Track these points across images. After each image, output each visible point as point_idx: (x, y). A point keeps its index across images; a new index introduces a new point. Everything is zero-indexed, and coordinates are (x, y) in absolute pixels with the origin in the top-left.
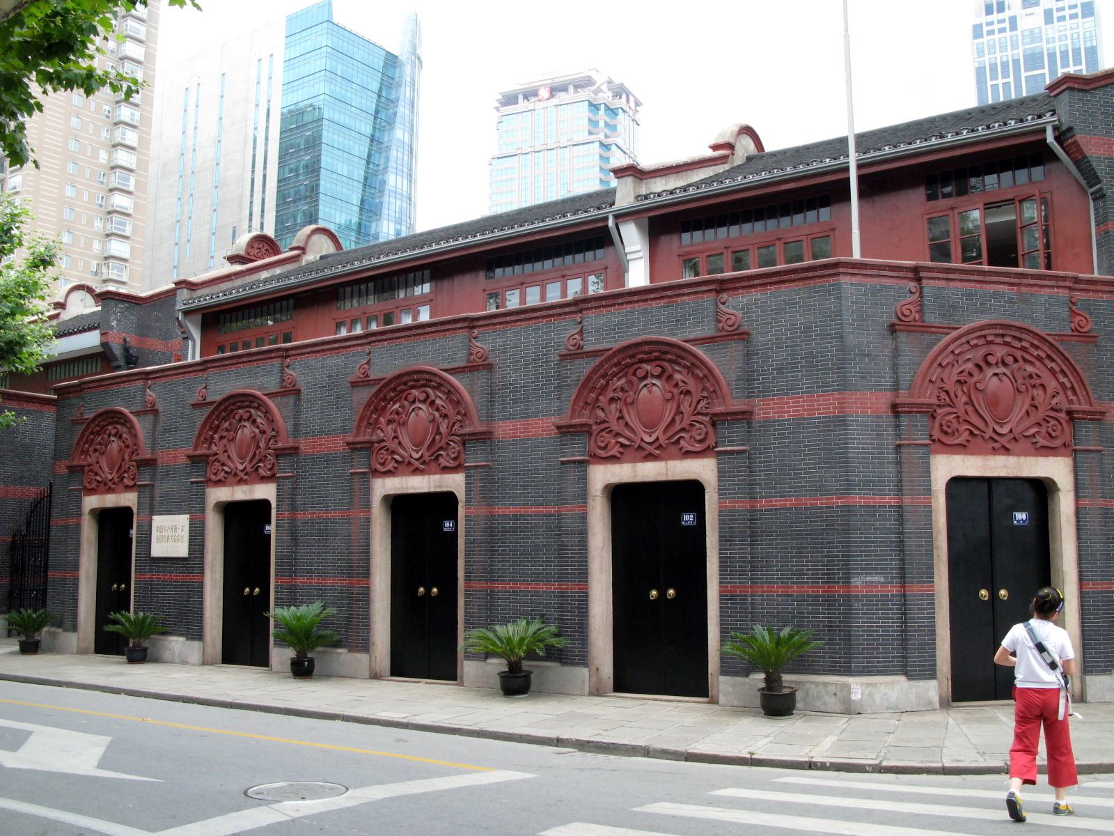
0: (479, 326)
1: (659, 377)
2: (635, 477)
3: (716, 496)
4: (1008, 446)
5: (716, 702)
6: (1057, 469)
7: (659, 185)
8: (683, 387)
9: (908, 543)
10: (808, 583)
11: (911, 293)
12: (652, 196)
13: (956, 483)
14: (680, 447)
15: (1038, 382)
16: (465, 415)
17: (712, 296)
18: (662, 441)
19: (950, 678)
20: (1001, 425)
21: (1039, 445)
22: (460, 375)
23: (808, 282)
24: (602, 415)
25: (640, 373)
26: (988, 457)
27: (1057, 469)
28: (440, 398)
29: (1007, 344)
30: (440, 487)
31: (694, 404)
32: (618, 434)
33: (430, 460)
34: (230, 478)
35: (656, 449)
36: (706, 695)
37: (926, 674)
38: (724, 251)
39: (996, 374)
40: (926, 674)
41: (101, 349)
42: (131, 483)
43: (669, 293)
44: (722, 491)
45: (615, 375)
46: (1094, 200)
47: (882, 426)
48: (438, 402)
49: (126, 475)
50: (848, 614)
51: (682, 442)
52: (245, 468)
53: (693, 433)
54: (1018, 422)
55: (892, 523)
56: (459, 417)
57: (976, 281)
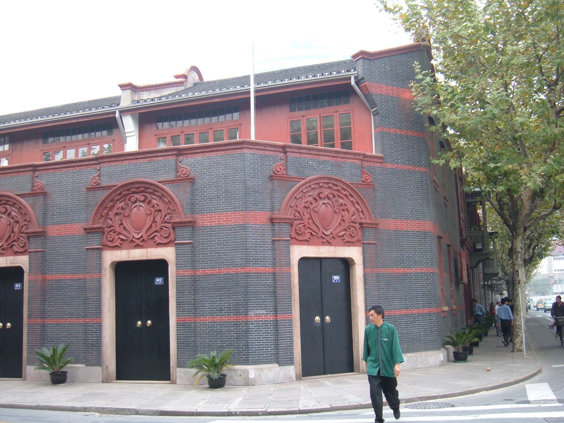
0: (39, 170)
1: (143, 202)
2: (129, 257)
3: (175, 268)
4: (330, 241)
5: (175, 383)
7: (145, 96)
8: (158, 208)
9: (279, 292)
10: (225, 315)
11: (282, 159)
12: (141, 101)
13: (304, 261)
14: (155, 241)
15: (345, 208)
16: (29, 221)
17: (174, 157)
18: (145, 237)
19: (301, 364)
20: (327, 230)
21: (345, 241)
22: (27, 198)
23: (226, 152)
24: (111, 222)
25: (133, 199)
28: (15, 211)
29: (330, 188)
30: (13, 263)
31: (163, 217)
32: (119, 233)
33: (7, 248)
35: (141, 242)
36: (169, 379)
37: (288, 363)
38: (181, 134)
39: (324, 204)
40: (288, 363)
43: (150, 155)
44: (178, 265)
45: (118, 200)
46: (374, 115)
47: (265, 230)
48: (13, 214)
50: (247, 331)
51: (156, 238)
53: (162, 233)
55: (271, 281)
56: (26, 223)
57: (315, 155)
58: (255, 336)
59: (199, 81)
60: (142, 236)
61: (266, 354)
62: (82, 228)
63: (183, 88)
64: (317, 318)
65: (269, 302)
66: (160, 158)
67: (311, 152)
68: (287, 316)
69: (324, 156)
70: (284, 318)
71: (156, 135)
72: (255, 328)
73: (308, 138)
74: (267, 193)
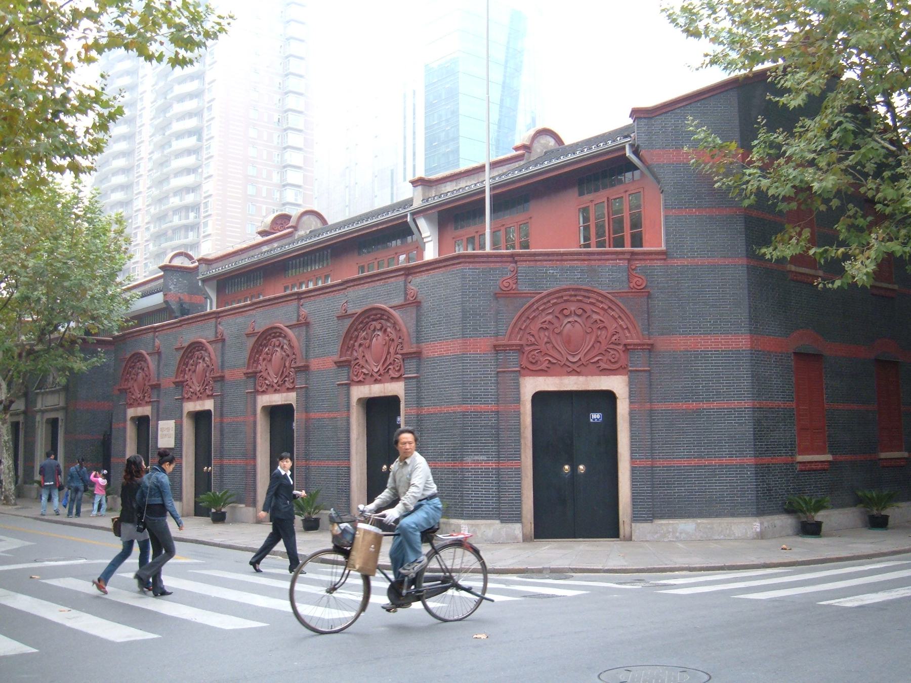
4: (578, 370)
6: (617, 384)
7: (449, 187)
13: (540, 398)
15: (601, 325)
19: (533, 522)
20: (574, 356)
21: (601, 368)
22: (294, 329)
23: (398, 278)
26: (563, 377)
27: (617, 384)
30: (287, 401)
33: (384, 373)
34: (270, 389)
37: (513, 520)
38: (476, 234)
39: (569, 322)
40: (513, 520)
41: (164, 306)
42: (291, 386)
48: (285, 347)
49: (207, 387)
50: (463, 480)
52: (379, 370)
53: (395, 366)
54: (584, 355)
57: (557, 260)
58: (471, 486)
59: (557, 146)
61: (485, 508)
62: (333, 361)
63: (522, 163)
64: (385, 467)
65: (492, 446)
66: (392, 279)
67: (550, 258)
68: (512, 463)
69: (570, 260)
70: (508, 466)
71: (454, 238)
72: (472, 477)
73: (631, 220)
74: (492, 314)
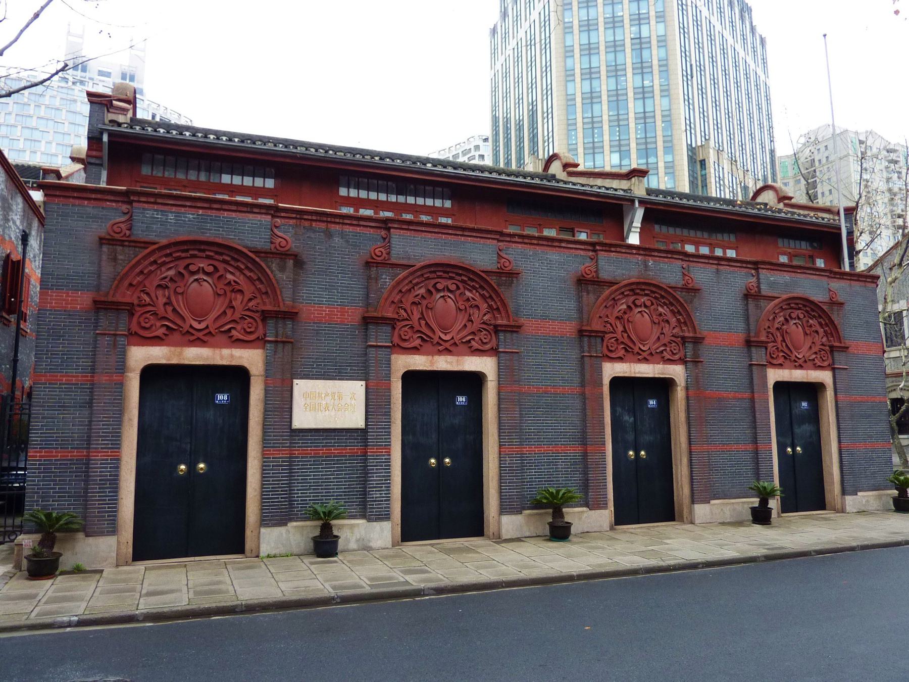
35: (204, 335)
60: (207, 327)
